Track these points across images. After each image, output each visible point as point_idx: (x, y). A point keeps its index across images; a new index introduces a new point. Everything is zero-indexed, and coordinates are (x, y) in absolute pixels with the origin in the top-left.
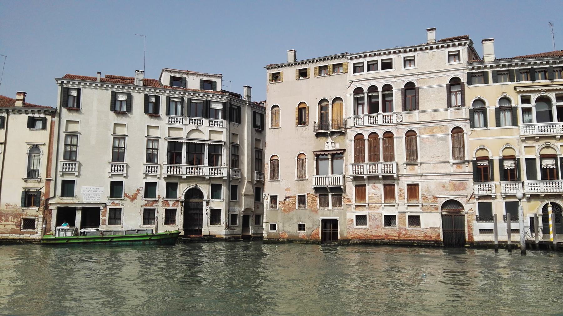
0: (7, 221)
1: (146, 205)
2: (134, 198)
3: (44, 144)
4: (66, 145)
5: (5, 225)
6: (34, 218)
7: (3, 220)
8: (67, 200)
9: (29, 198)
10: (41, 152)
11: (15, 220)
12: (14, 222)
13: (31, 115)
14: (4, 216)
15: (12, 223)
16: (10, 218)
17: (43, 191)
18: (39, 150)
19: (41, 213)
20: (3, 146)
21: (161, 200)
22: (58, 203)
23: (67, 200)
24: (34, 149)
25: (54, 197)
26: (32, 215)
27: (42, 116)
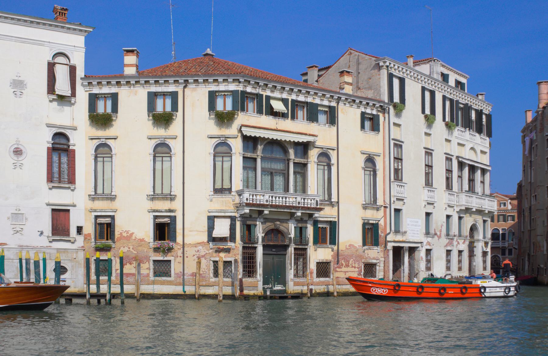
0: (347, 266)
1: (446, 246)
2: (439, 237)
3: (379, 156)
4: (395, 158)
5: (345, 272)
6: (374, 261)
7: (342, 264)
8: (399, 238)
9: (371, 234)
10: (377, 167)
11: (357, 265)
12: (355, 267)
13: (363, 111)
14: (344, 259)
15: (353, 269)
16: (350, 262)
17: (382, 223)
18: (374, 164)
19: (382, 254)
20: (336, 151)
21: (455, 238)
22: (394, 242)
23: (399, 238)
24: (370, 160)
25: (389, 233)
26: (374, 259)
27: (374, 112)
